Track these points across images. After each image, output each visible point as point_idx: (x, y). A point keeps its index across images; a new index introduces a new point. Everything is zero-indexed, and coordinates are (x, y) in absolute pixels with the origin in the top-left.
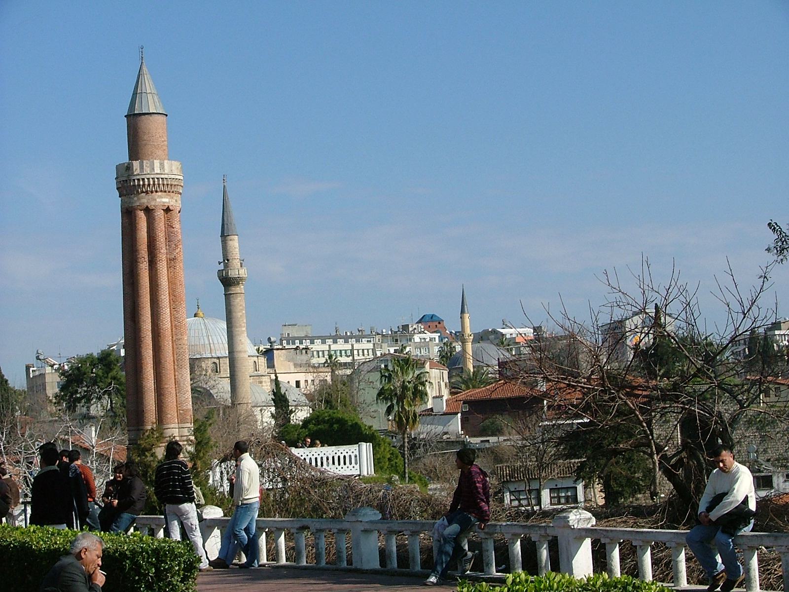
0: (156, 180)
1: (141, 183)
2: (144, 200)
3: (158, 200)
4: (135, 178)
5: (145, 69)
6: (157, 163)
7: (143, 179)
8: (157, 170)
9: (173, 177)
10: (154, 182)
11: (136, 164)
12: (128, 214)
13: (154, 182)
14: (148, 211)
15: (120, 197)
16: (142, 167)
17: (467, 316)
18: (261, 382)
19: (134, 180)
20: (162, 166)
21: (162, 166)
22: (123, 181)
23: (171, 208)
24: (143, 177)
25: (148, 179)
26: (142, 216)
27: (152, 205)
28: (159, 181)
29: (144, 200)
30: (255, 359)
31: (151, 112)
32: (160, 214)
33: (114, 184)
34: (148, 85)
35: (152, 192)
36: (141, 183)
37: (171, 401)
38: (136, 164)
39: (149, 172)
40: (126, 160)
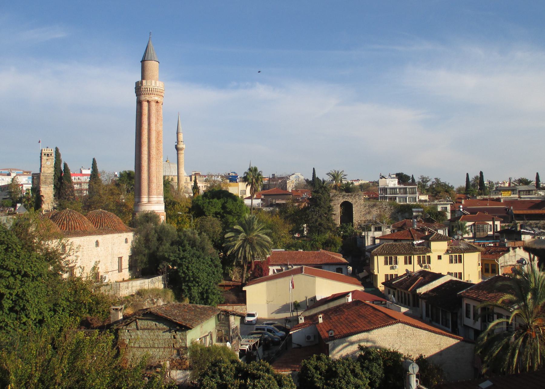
0: (153, 89)
1: (146, 90)
5: (151, 43)
6: (153, 82)
7: (147, 88)
8: (153, 85)
9: (160, 88)
10: (152, 90)
12: (139, 103)
13: (152, 90)
14: (148, 102)
19: (143, 88)
20: (155, 83)
21: (155, 83)
23: (159, 102)
26: (145, 104)
27: (150, 99)
28: (154, 89)
29: (147, 98)
30: (186, 177)
32: (153, 104)
36: (146, 90)
38: (144, 82)
40: (139, 79)
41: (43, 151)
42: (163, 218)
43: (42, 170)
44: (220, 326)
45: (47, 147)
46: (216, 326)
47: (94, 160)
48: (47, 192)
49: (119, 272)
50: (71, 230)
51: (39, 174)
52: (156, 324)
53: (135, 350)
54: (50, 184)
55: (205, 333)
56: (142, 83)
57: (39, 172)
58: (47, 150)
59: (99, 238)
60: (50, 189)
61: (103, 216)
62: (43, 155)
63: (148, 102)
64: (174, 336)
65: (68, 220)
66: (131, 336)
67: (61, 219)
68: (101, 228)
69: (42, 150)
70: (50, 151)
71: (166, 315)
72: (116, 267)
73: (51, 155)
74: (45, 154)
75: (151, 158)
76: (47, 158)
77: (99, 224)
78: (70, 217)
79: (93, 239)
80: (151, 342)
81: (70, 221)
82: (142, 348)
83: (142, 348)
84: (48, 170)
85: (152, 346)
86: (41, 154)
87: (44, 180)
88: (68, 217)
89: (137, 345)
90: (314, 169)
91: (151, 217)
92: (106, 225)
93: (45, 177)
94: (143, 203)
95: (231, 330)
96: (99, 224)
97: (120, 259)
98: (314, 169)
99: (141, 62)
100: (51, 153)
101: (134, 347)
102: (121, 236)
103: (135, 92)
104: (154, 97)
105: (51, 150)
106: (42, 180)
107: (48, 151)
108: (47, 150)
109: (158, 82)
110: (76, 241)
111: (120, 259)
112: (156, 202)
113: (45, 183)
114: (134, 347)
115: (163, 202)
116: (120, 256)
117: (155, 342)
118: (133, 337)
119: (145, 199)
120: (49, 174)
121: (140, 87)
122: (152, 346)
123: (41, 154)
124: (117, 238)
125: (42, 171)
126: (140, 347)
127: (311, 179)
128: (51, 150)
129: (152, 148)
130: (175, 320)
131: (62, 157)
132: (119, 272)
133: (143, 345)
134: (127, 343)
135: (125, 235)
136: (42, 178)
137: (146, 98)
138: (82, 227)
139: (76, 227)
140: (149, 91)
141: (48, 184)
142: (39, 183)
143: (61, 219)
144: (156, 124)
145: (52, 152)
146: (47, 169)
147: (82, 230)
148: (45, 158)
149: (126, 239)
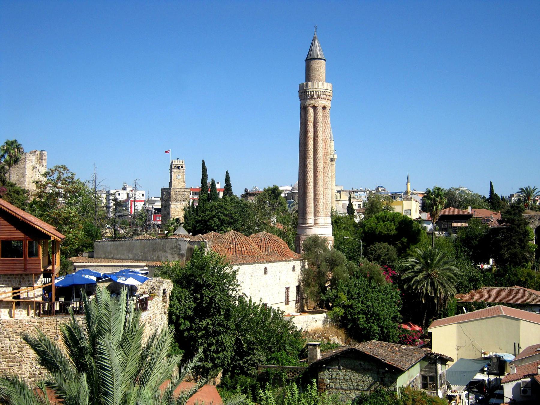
2: (313, 102)
3: (320, 102)
4: (308, 90)
6: (320, 83)
7: (313, 91)
11: (310, 84)
12: (304, 109)
15: (300, 101)
16: (313, 85)
17: (409, 184)
18: (338, 203)
19: (308, 92)
20: (323, 84)
21: (323, 84)
22: (303, 92)
23: (326, 106)
24: (313, 90)
25: (316, 91)
26: (311, 110)
27: (316, 105)
29: (313, 102)
31: (318, 58)
32: (320, 109)
33: (297, 94)
34: (317, 45)
35: (317, 98)
36: (312, 93)
37: (321, 205)
38: (310, 84)
39: (316, 88)
40: (304, 81)
41: (174, 163)
42: (330, 244)
43: (172, 184)
44: (425, 371)
45: (178, 159)
46: (421, 370)
47: (227, 173)
48: (177, 210)
49: (286, 304)
50: (238, 255)
51: (170, 189)
52: (361, 364)
53: (335, 391)
54: (180, 201)
55: (412, 377)
56: (307, 86)
57: (168, 187)
58: (177, 162)
59: (267, 265)
60: (180, 207)
61: (268, 239)
62: (173, 167)
63: (315, 108)
64: (382, 378)
65: (234, 243)
66: (332, 376)
67: (227, 242)
68: (266, 253)
69: (172, 162)
70: (181, 163)
71: (373, 354)
72: (284, 299)
73: (182, 167)
74: (175, 167)
75: (318, 173)
76: (178, 170)
77: (264, 249)
78: (236, 240)
79: (262, 266)
80: (355, 384)
81: (237, 245)
82: (344, 389)
83: (344, 389)
84: (178, 185)
85: (355, 388)
86: (171, 166)
87: (174, 196)
88: (234, 240)
89: (338, 386)
90: (491, 183)
91: (317, 242)
92: (272, 250)
93: (175, 192)
94: (308, 225)
95: (438, 376)
96: (264, 249)
97: (288, 289)
98: (491, 183)
99: (305, 61)
100: (181, 166)
101: (335, 388)
102: (288, 263)
103: (299, 96)
104: (322, 101)
105: (182, 162)
106: (172, 196)
107: (179, 163)
108: (177, 162)
109: (325, 84)
110: (243, 267)
111: (288, 289)
112: (323, 224)
113: (175, 199)
114: (335, 388)
115: (330, 224)
116: (288, 286)
117: (359, 384)
118: (334, 377)
119: (310, 222)
120: (179, 190)
121: (306, 90)
122: (355, 388)
123: (171, 166)
124: (284, 265)
125: (172, 186)
126: (342, 388)
127: (487, 196)
128: (182, 162)
129: (319, 161)
130: (383, 360)
131: (208, 172)
132: (286, 304)
133: (345, 386)
134: (327, 383)
135: (292, 263)
136: (172, 193)
137: (312, 102)
138: (250, 252)
139: (243, 252)
140: (316, 94)
141: (178, 201)
142: (169, 200)
143: (227, 242)
144: (324, 132)
145: (183, 164)
146: (177, 183)
147: (250, 255)
148: (175, 170)
149: (294, 267)
